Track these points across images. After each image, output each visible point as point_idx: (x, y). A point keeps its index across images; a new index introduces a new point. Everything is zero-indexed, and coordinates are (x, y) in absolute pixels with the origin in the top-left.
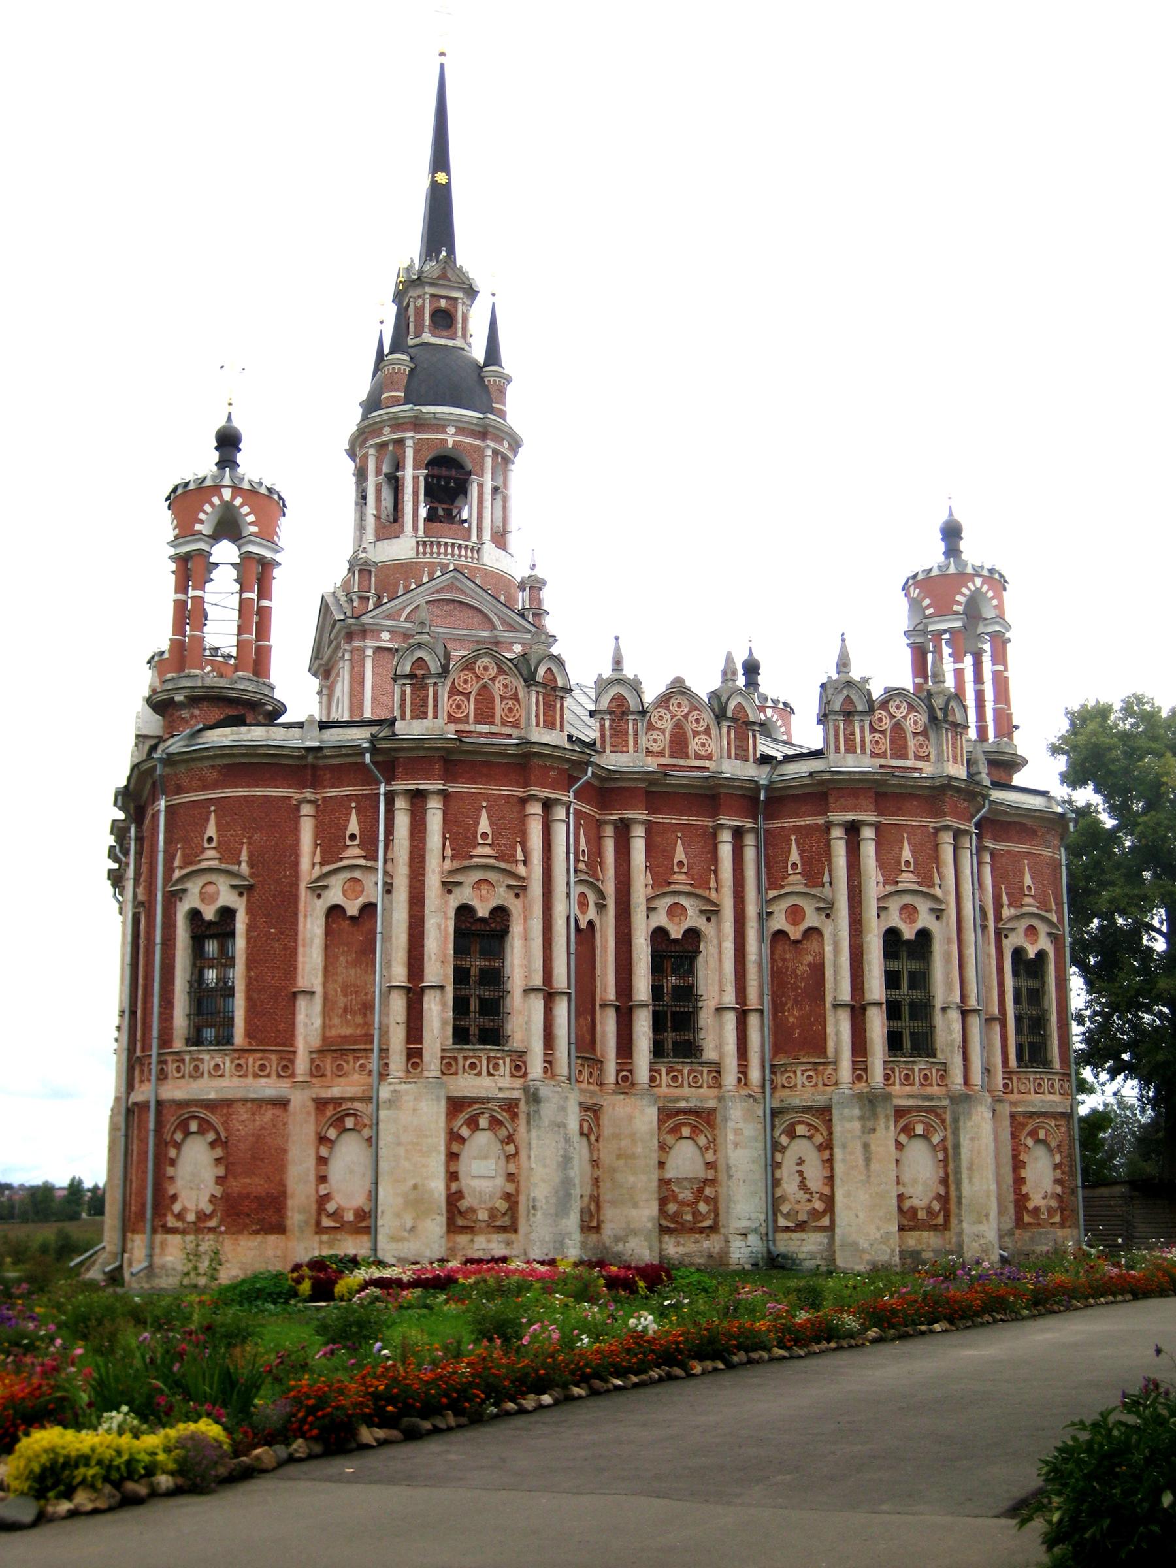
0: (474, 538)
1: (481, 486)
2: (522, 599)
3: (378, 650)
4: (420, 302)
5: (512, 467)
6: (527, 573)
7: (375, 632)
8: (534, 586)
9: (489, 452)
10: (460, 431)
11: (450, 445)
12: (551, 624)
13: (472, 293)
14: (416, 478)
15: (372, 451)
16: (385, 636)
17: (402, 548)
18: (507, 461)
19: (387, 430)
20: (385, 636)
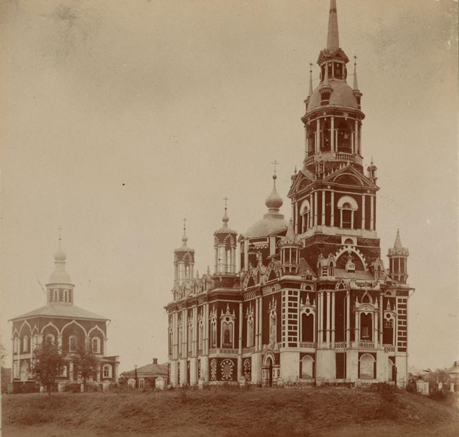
0: (353, 153)
1: (354, 134)
2: (366, 173)
3: (326, 192)
4: (330, 65)
5: (362, 127)
6: (370, 165)
7: (326, 186)
8: (372, 170)
9: (357, 122)
10: (350, 115)
11: (346, 119)
12: (378, 183)
13: (347, 61)
14: (335, 132)
15: (318, 121)
16: (329, 187)
17: (331, 156)
18: (360, 124)
19: (325, 114)
20: (329, 187)
